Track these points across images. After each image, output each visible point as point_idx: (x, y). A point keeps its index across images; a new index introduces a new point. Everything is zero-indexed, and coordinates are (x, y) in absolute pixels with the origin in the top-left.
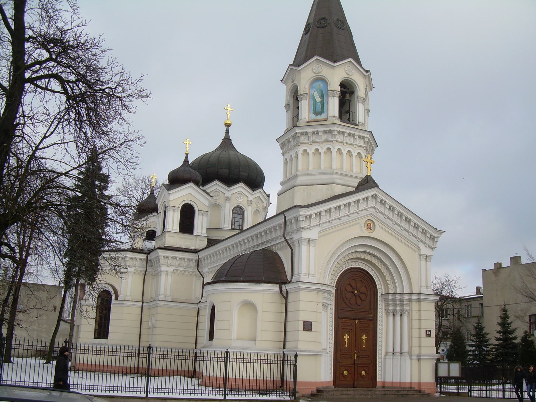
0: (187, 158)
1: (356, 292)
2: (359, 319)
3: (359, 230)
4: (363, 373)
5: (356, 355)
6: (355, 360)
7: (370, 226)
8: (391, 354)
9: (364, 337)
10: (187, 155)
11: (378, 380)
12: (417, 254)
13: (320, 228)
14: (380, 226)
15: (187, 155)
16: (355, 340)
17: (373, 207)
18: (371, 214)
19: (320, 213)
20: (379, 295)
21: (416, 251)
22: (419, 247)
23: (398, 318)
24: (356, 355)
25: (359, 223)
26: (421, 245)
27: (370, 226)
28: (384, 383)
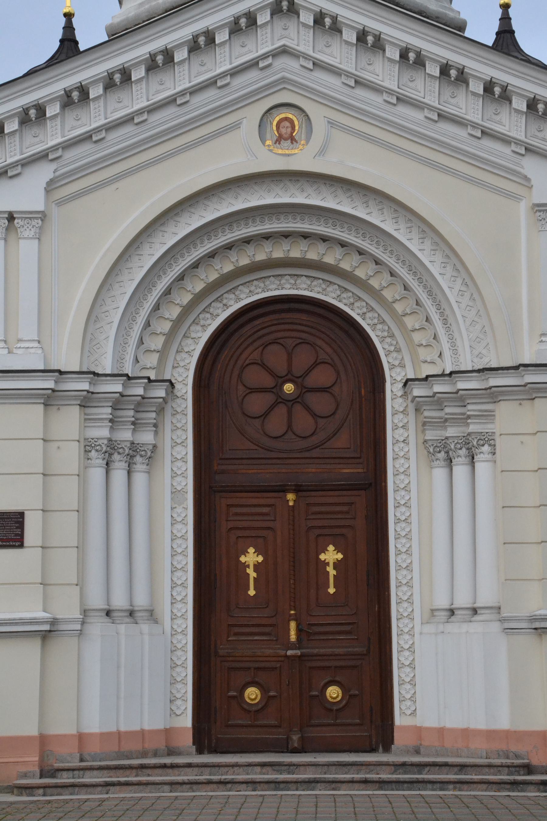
0: (69, 28)
1: (289, 388)
2: (298, 490)
3: (242, 151)
4: (333, 692)
5: (293, 625)
6: (290, 646)
7: (284, 124)
8: (444, 615)
9: (331, 555)
10: (69, 16)
11: (399, 720)
12: (523, 207)
13: (54, 166)
14: (331, 123)
15: (69, 16)
16: (293, 569)
17: (284, 51)
18: (284, 80)
19: (41, 110)
20: (392, 390)
21: (517, 198)
22: (527, 179)
23: (460, 471)
24: (293, 625)
25: (236, 126)
26: (530, 166)
27: (284, 124)
28: (419, 730)
